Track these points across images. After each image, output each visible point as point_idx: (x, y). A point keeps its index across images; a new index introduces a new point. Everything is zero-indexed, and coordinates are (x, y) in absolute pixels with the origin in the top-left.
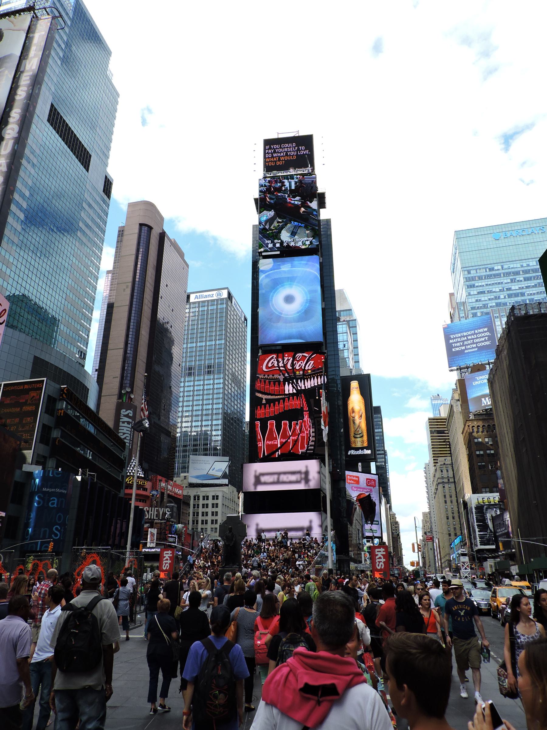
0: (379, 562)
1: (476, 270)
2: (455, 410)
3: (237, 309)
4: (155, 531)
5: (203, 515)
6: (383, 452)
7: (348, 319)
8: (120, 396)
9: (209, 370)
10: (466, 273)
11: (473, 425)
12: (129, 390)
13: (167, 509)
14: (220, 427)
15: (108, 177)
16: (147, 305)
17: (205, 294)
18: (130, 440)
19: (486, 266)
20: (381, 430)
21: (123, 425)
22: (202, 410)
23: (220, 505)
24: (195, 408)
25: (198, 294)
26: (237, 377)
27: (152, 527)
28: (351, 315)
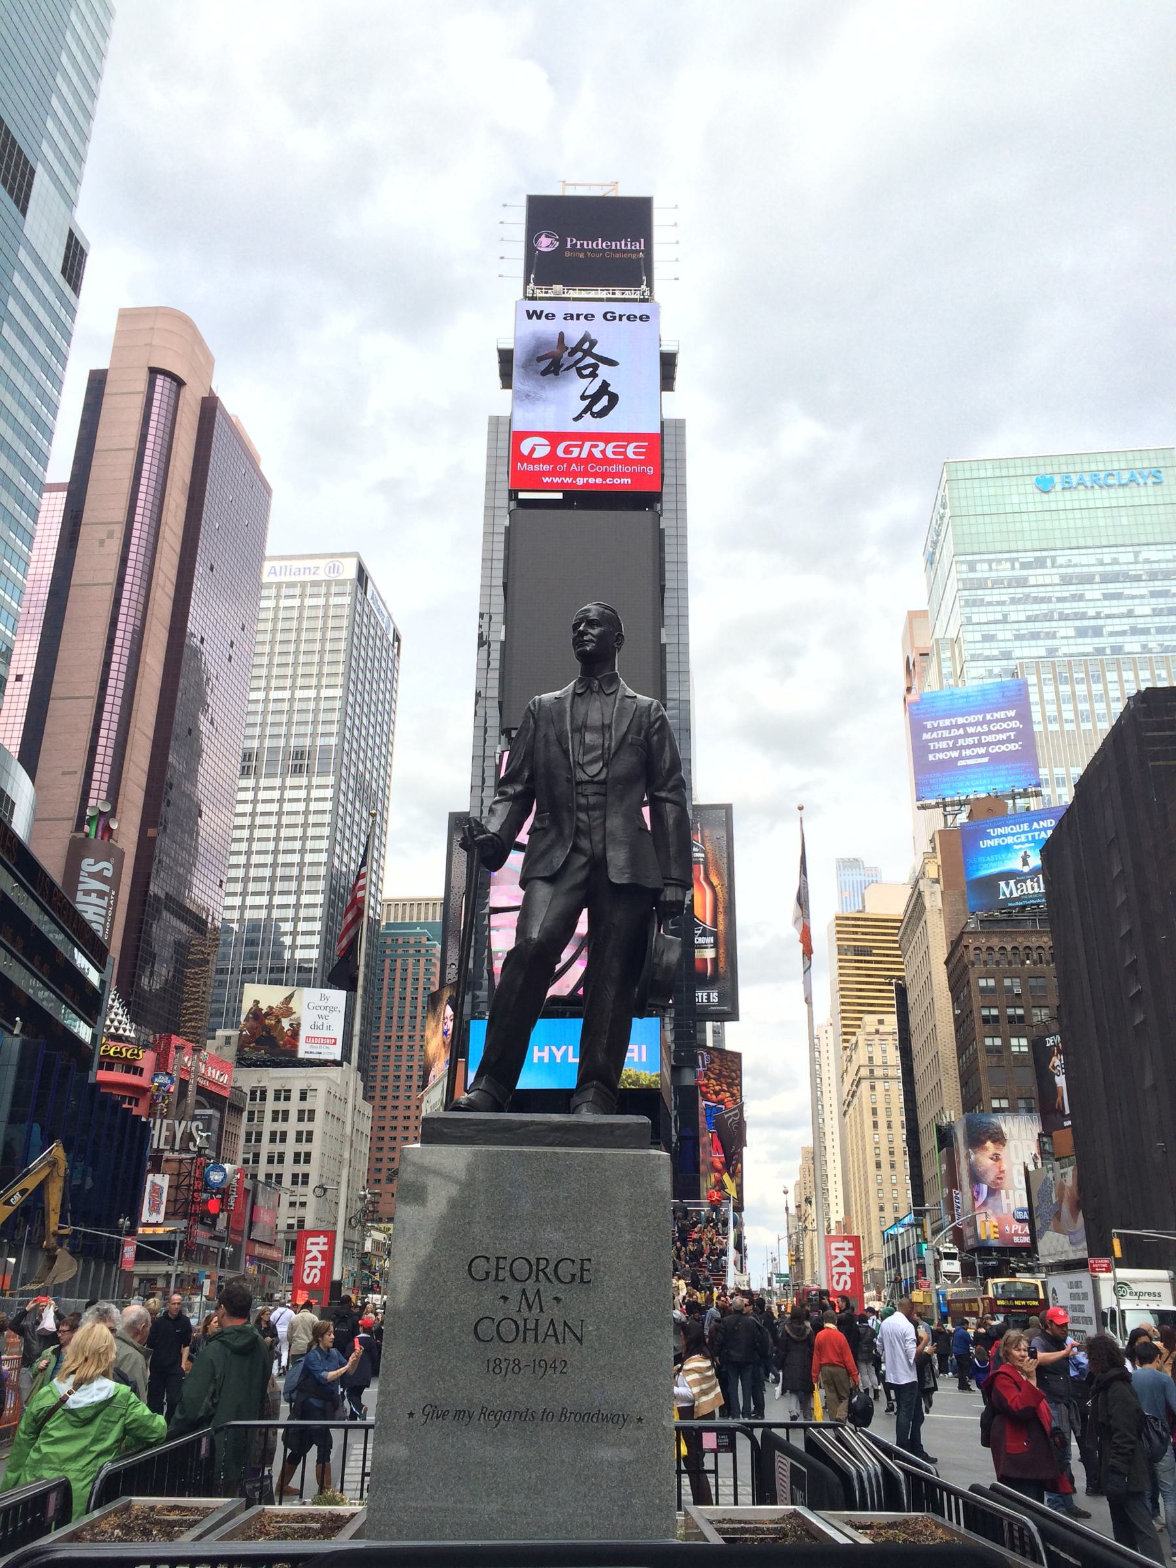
1: (990, 562)
2: (927, 905)
3: (379, 610)
4: (162, 1181)
5: (273, 1140)
8: (81, 821)
9: (298, 762)
10: (965, 567)
11: (977, 944)
12: (106, 808)
13: (195, 1124)
14: (318, 912)
15: (77, 235)
16: (163, 589)
17: (296, 564)
19: (1014, 555)
22: (274, 865)
23: (319, 1115)
24: (255, 859)
26: (370, 785)
27: (157, 1169)
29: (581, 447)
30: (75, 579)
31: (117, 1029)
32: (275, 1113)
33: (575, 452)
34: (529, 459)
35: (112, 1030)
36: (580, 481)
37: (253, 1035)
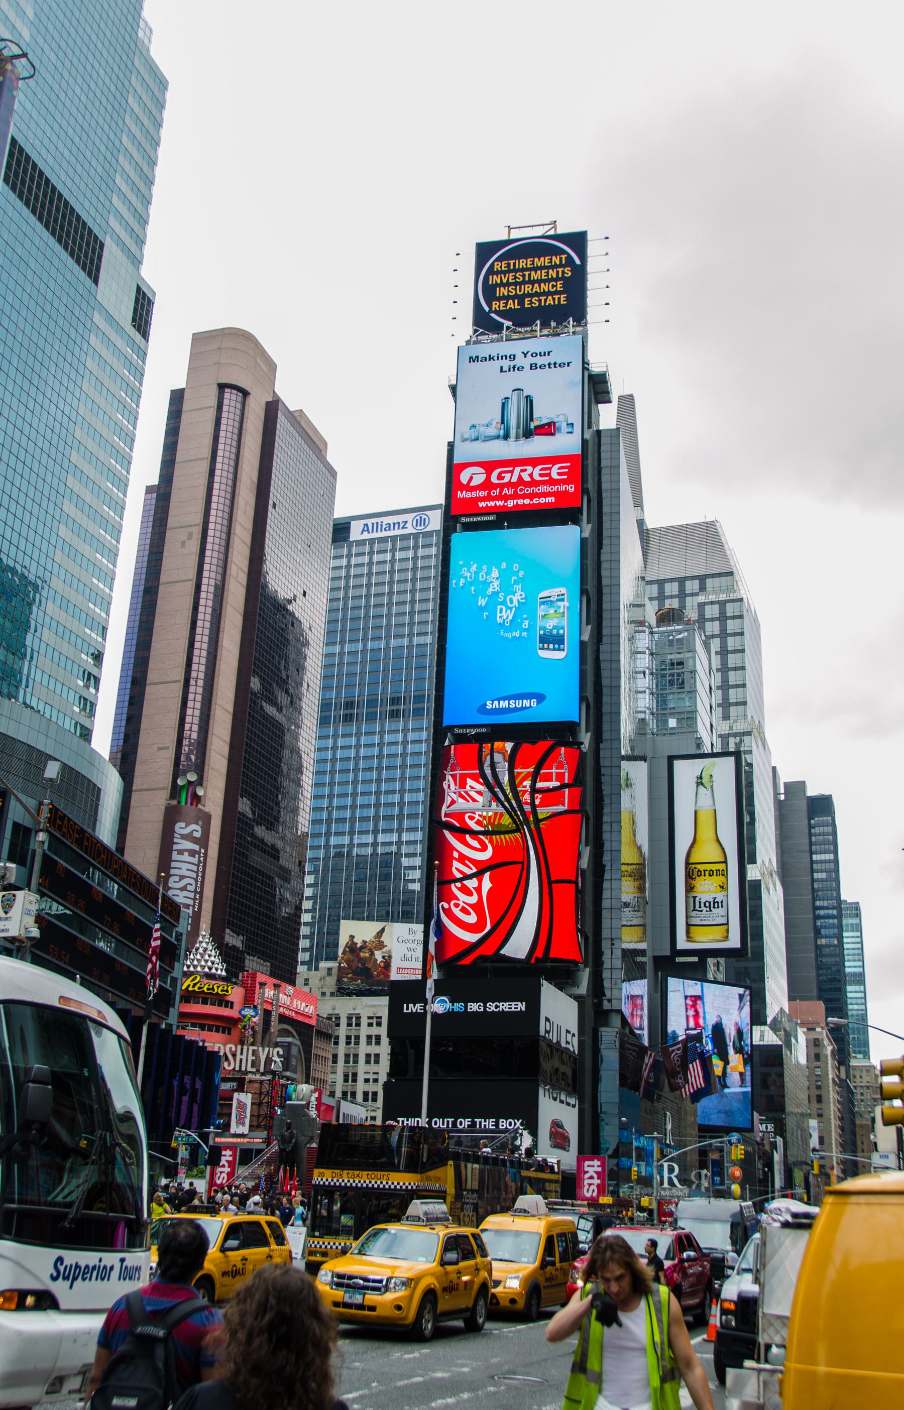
0: (590, 1185)
4: (246, 1098)
6: (835, 912)
7: (723, 597)
8: (175, 791)
9: (395, 708)
12: (192, 777)
13: (276, 1050)
15: (144, 289)
17: (386, 520)
18: (195, 892)
20: (831, 857)
21: (180, 858)
25: (369, 522)
27: (241, 1089)
28: (731, 589)
29: (512, 472)
30: (163, 578)
31: (210, 969)
32: (369, 1037)
33: (507, 477)
34: (468, 488)
35: (207, 970)
36: (511, 503)
37: (350, 967)
